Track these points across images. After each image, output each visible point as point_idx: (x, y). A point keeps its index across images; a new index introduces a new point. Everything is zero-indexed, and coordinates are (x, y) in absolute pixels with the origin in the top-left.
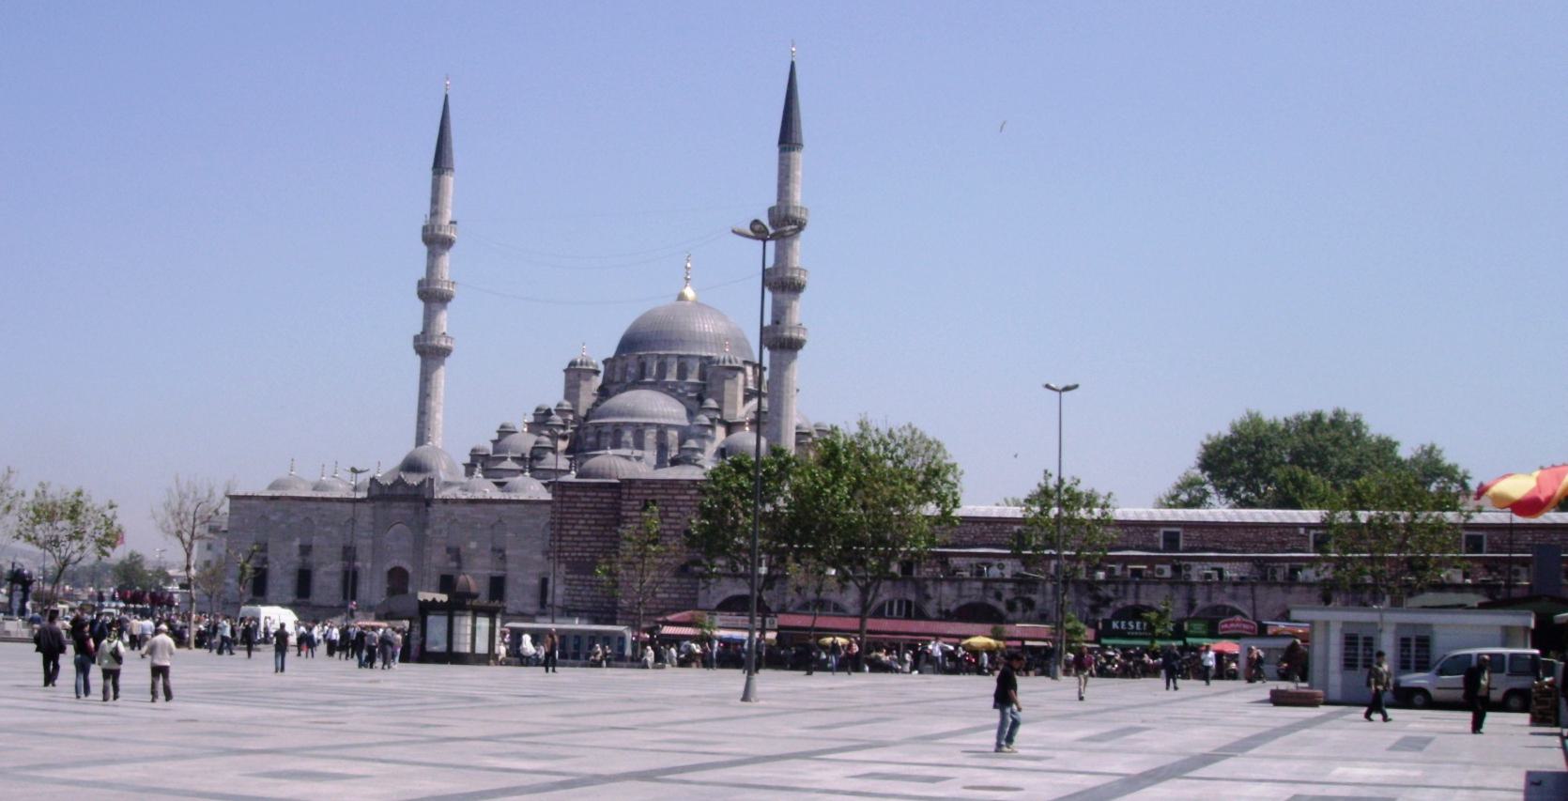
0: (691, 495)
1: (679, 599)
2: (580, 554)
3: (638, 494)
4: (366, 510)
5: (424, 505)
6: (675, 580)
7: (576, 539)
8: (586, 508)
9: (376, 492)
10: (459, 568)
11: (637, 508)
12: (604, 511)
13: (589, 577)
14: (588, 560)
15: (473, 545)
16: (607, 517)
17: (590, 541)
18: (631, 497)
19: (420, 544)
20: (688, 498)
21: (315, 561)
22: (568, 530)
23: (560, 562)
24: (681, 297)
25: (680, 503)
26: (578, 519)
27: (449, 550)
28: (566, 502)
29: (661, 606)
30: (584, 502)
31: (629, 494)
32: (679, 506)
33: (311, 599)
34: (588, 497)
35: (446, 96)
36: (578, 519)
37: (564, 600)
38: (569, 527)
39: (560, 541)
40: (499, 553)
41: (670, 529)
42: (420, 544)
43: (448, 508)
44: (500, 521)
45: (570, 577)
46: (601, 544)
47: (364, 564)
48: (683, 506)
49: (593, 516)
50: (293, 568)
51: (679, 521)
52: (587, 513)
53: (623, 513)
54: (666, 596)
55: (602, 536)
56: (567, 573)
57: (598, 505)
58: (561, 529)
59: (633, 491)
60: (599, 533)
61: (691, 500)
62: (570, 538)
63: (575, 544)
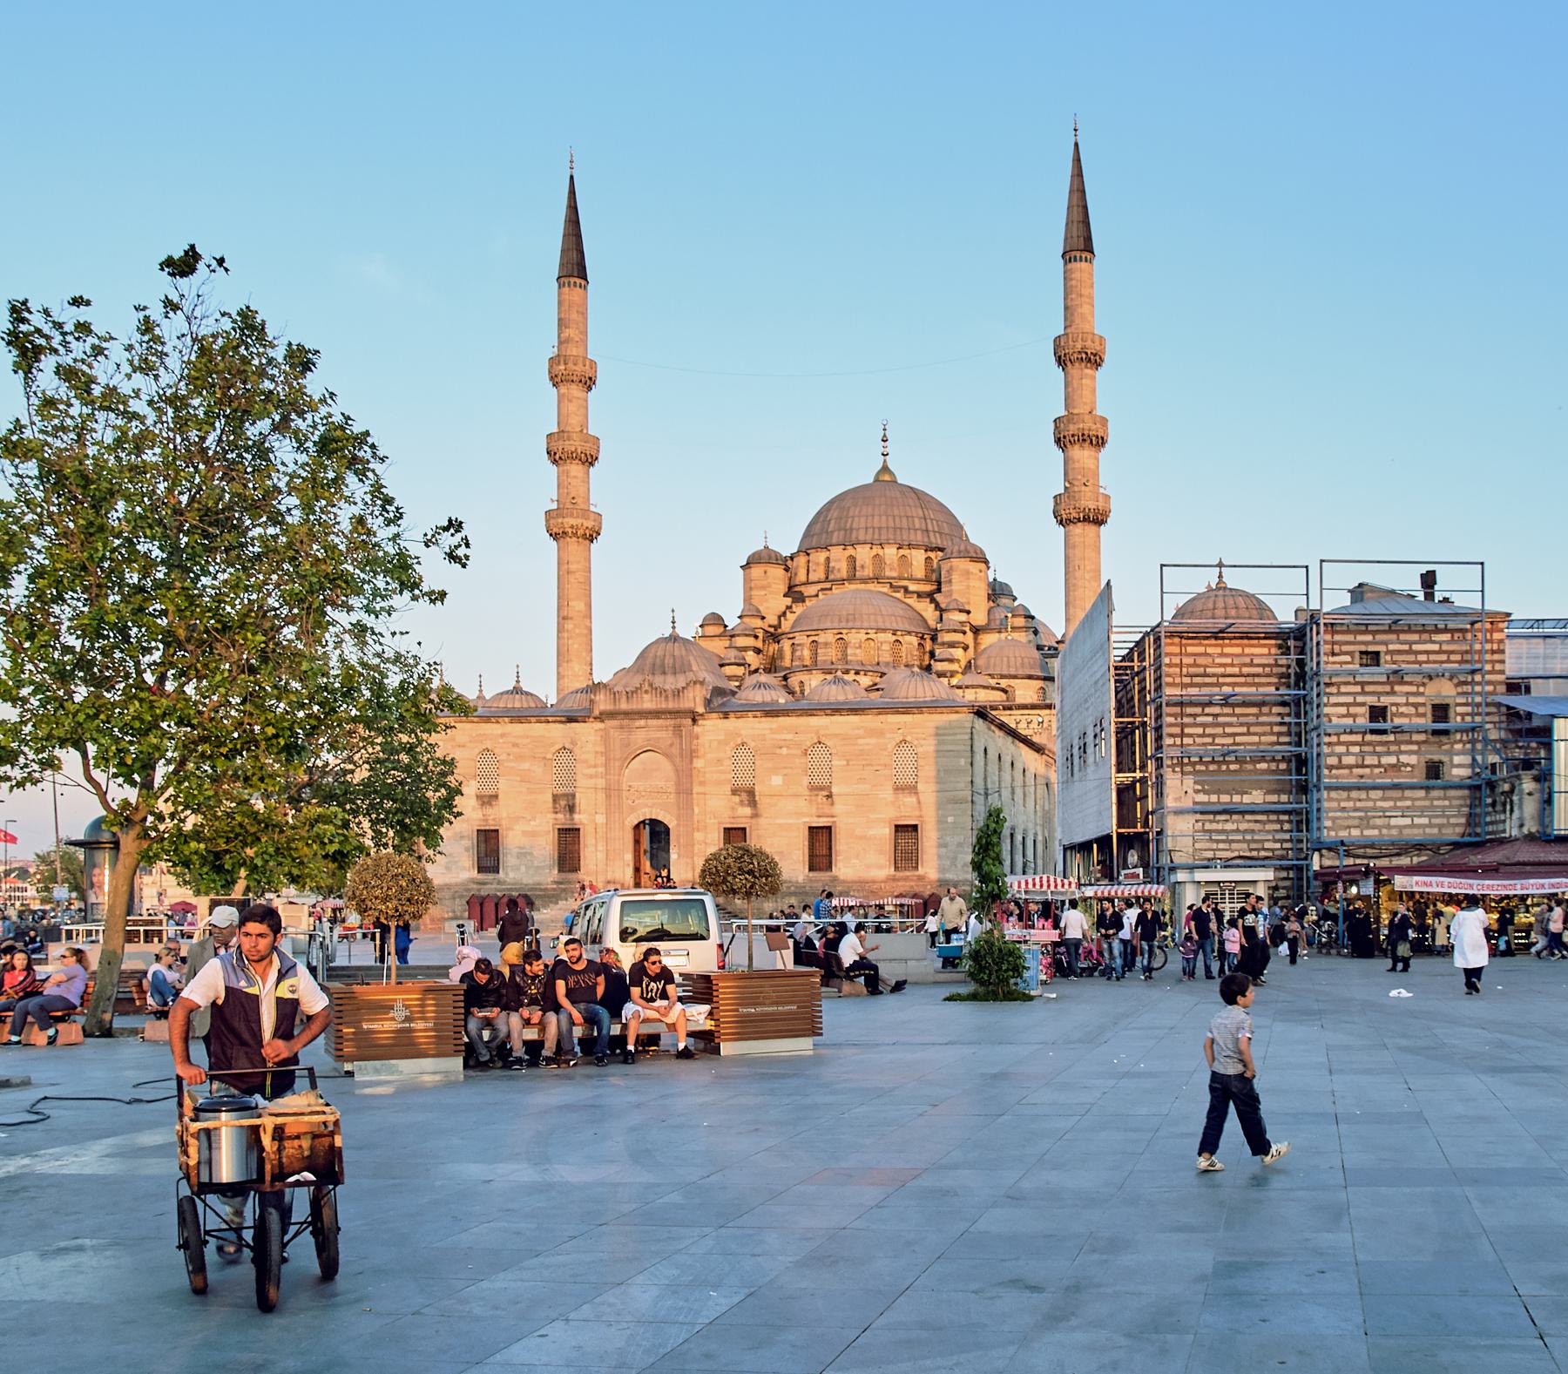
0: (1440, 643)
5: (689, 721)
7: (1208, 731)
10: (755, 816)
14: (1232, 767)
15: (777, 780)
17: (1234, 735)
18: (1337, 649)
20: (1436, 647)
21: (504, 815)
22: (1195, 716)
25: (1422, 658)
27: (734, 792)
28: (1189, 666)
30: (1221, 665)
34: (1227, 655)
37: (1195, 841)
39: (1182, 735)
41: (1407, 704)
46: (1256, 739)
48: (1428, 662)
54: (1408, 821)
56: (1197, 792)
57: (1246, 670)
59: (1337, 638)
60: (1252, 719)
62: (1200, 730)
63: (1209, 740)
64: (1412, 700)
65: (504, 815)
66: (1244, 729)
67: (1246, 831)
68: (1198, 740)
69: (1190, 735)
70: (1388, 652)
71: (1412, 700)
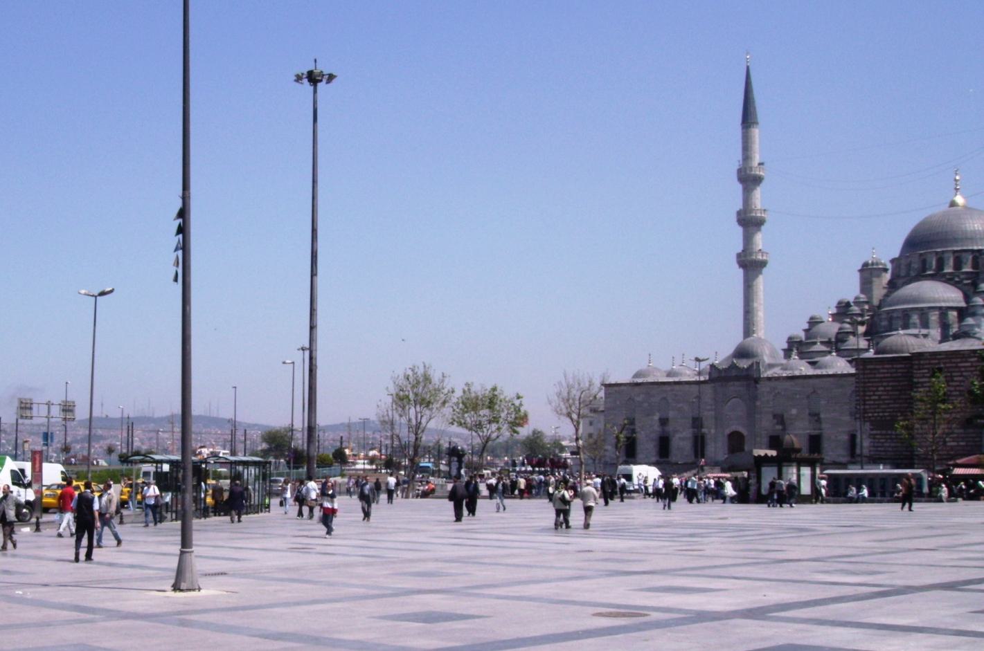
0: (971, 362)
1: (967, 446)
2: (881, 414)
3: (926, 364)
4: (708, 389)
6: (961, 431)
7: (877, 402)
8: (885, 377)
9: (715, 375)
10: (784, 429)
11: (926, 375)
12: (900, 379)
13: (889, 432)
14: (888, 418)
15: (794, 411)
16: (901, 384)
17: (888, 404)
18: (921, 367)
19: (752, 413)
20: (969, 364)
21: (671, 429)
22: (870, 396)
23: (865, 421)
24: (953, 204)
25: (963, 369)
26: (878, 387)
27: (775, 416)
28: (867, 374)
29: (952, 453)
31: (920, 364)
32: (962, 372)
33: (670, 459)
35: (748, 68)
36: (878, 387)
37: (870, 451)
38: (872, 393)
39: (864, 404)
40: (815, 417)
41: (956, 391)
42: (752, 413)
43: (772, 384)
44: (814, 392)
45: (874, 432)
47: (709, 430)
48: (966, 371)
49: (891, 384)
50: (655, 436)
51: (962, 384)
52: (885, 382)
53: (915, 380)
55: (899, 399)
56: (872, 430)
58: (865, 396)
59: (922, 362)
61: (972, 366)
62: (872, 402)
64: (958, 388)
65: (671, 429)
66: (892, 401)
67: (893, 447)
68: (872, 407)
69: (867, 405)
70: (946, 367)
71: (958, 388)
